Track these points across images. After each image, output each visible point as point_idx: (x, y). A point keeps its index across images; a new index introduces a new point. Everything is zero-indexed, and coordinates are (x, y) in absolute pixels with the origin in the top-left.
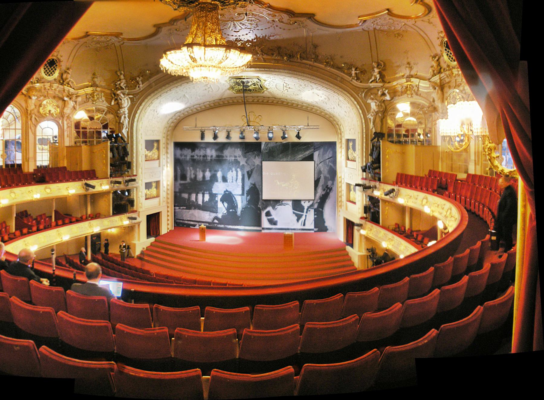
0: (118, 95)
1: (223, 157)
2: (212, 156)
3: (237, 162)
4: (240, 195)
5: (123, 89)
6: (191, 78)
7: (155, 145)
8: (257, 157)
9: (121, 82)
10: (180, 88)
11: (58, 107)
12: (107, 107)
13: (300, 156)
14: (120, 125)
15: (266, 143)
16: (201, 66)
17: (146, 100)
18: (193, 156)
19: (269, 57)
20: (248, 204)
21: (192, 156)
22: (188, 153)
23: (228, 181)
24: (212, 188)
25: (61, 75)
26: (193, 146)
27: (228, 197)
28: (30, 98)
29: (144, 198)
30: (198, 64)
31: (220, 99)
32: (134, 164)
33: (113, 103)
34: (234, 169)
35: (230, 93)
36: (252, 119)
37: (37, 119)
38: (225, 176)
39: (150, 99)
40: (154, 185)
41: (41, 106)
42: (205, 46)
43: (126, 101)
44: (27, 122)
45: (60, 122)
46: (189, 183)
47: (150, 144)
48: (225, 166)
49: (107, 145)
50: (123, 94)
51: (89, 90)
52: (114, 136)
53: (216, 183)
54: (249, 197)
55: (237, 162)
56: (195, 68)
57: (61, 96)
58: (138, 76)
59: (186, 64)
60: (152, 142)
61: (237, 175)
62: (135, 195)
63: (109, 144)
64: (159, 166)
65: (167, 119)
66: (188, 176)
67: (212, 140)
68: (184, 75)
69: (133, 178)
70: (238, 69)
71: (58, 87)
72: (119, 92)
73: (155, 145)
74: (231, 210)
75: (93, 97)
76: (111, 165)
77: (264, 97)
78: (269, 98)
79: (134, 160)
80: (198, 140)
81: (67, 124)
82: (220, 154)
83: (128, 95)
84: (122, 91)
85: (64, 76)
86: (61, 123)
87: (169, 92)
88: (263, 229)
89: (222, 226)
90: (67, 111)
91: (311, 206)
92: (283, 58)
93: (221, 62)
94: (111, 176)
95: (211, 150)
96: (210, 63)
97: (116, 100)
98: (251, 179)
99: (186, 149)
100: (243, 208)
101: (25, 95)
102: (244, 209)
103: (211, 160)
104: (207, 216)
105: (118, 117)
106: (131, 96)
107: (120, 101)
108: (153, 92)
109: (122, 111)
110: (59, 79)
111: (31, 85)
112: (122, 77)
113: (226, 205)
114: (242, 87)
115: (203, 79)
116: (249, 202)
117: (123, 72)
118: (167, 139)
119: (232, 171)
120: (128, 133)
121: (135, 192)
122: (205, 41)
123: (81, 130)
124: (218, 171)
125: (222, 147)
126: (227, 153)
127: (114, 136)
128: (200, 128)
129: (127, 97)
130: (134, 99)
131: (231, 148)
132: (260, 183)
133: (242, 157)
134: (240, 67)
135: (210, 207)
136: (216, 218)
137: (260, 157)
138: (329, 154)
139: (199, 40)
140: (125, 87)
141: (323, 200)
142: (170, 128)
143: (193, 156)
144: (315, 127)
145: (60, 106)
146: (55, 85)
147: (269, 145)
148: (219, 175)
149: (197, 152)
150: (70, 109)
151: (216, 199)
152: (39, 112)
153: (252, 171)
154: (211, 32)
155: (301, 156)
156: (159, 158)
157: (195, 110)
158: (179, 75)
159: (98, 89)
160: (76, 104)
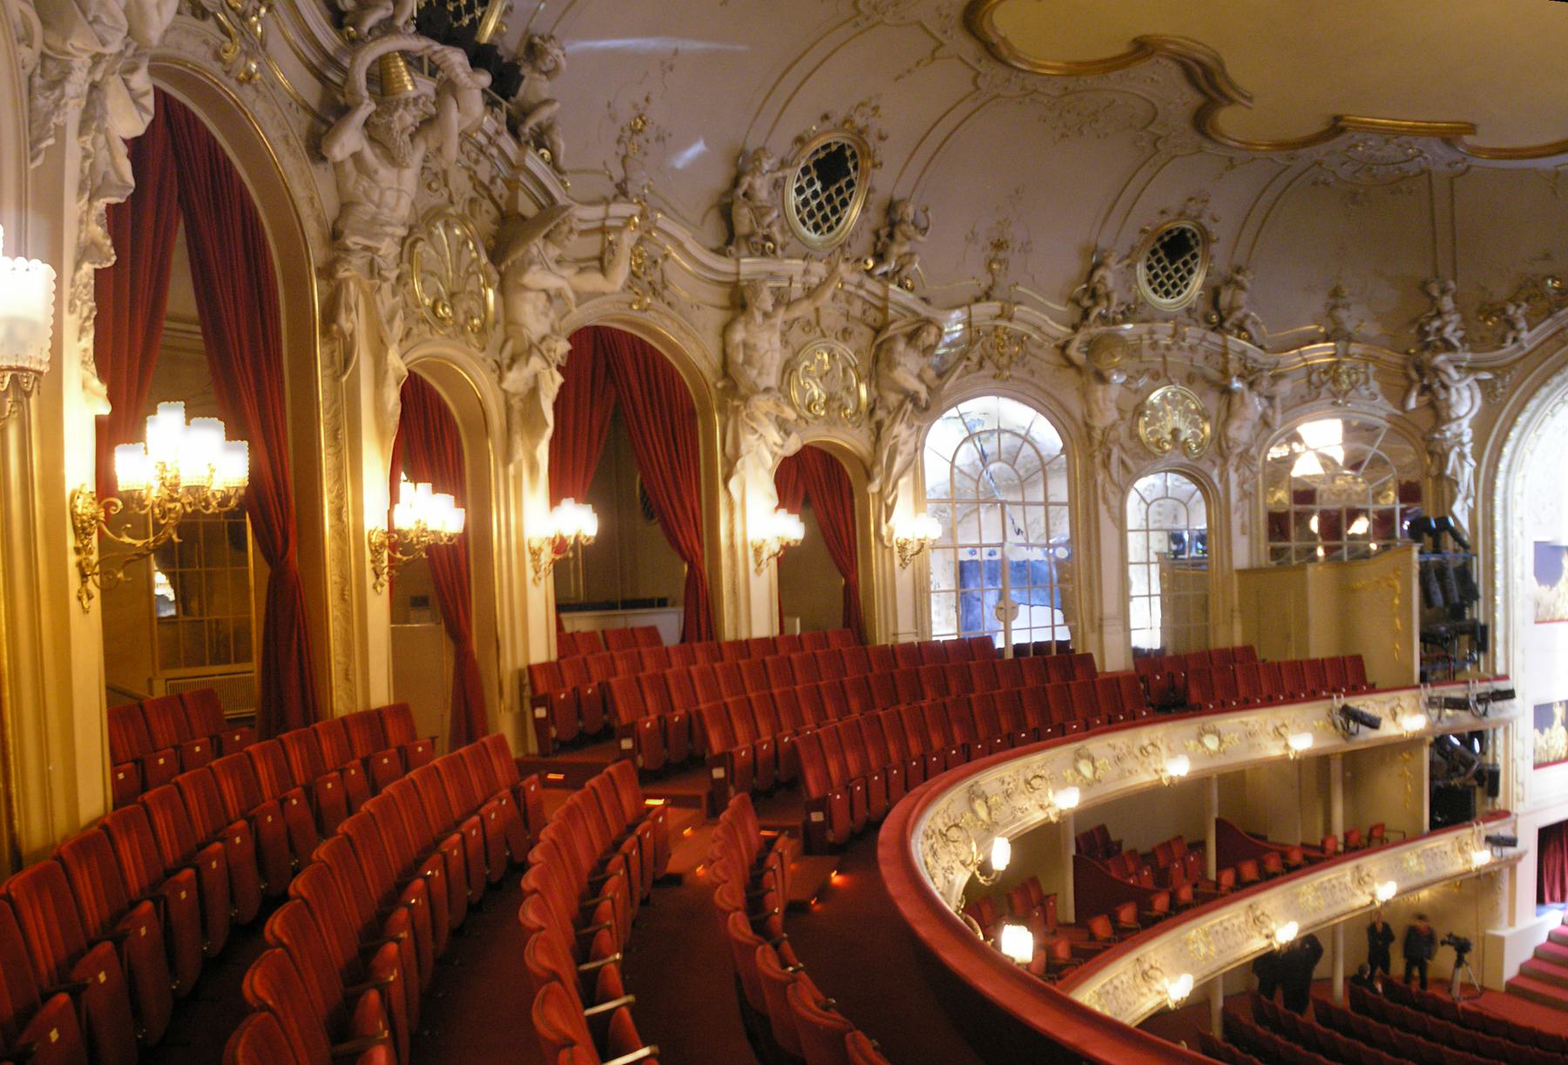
11: (1206, 418)
12: (1390, 418)
14: (1446, 486)
25: (1213, 294)
28: (1102, 378)
33: (1412, 403)
37: (1129, 462)
41: (1142, 414)
44: (1089, 476)
45: (1215, 474)
49: (1409, 564)
57: (1213, 374)
71: (1203, 339)
81: (1241, 484)
85: (1225, 299)
86: (1216, 480)
90: (1240, 432)
101: (1079, 370)
105: (1431, 453)
109: (1449, 431)
110: (1203, 307)
111: (1103, 329)
120: (1472, 515)
145: (1214, 413)
146: (1193, 333)
150: (1249, 424)
152: (1133, 435)
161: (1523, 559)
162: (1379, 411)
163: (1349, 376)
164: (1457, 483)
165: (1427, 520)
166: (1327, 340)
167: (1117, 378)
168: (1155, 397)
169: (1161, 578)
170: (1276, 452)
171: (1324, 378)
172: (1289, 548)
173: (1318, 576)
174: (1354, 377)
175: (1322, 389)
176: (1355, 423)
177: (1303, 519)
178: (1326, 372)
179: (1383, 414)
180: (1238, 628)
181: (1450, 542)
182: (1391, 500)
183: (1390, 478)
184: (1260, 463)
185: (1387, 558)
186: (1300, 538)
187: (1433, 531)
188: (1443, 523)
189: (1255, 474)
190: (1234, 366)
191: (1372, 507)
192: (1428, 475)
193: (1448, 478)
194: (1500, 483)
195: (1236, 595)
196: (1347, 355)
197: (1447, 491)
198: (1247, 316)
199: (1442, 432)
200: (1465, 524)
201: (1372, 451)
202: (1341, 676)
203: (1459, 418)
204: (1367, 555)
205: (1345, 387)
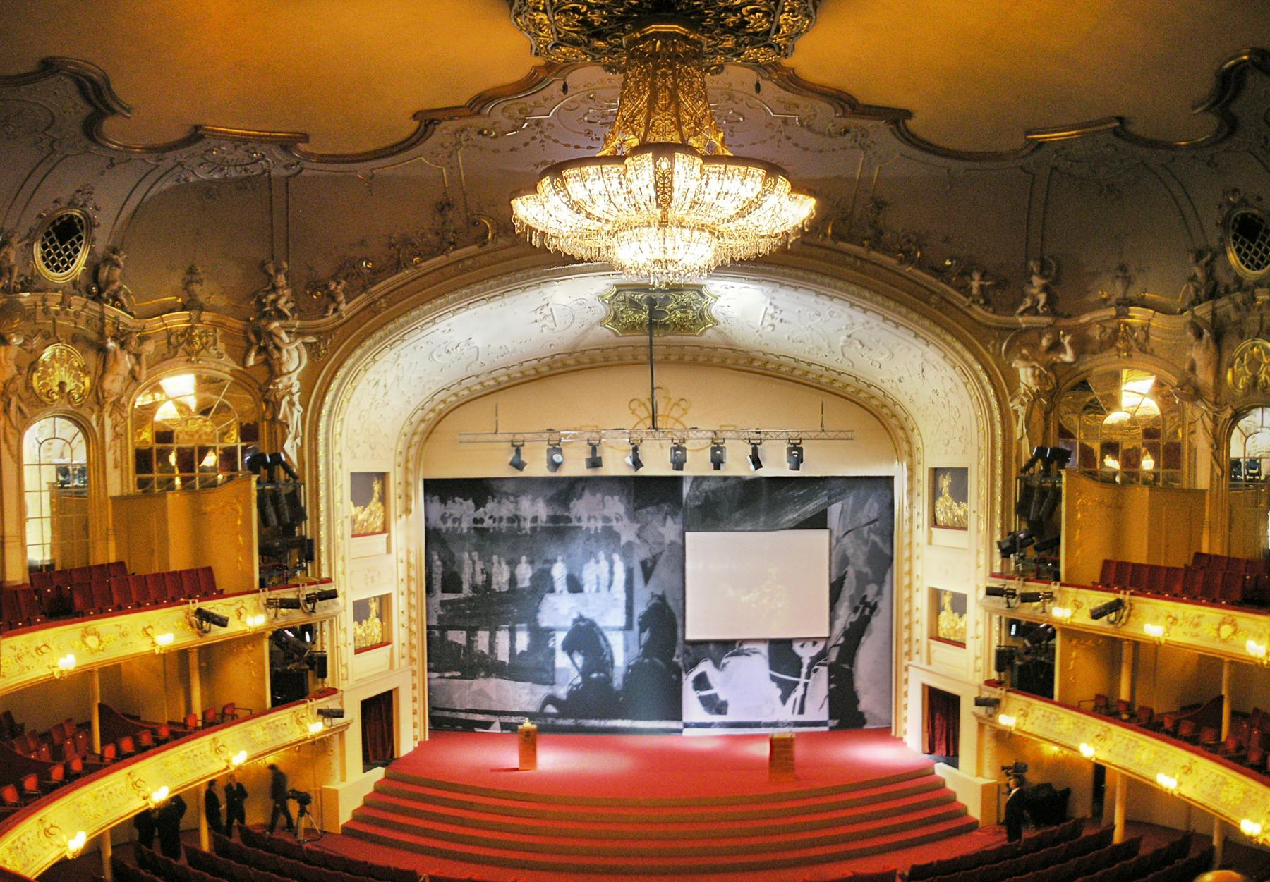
0: (271, 335)
1: (569, 520)
2: (535, 519)
3: (610, 535)
4: (620, 629)
5: (285, 317)
7: (377, 487)
8: (669, 520)
12: (233, 373)
13: (791, 516)
14: (279, 428)
17: (359, 352)
18: (482, 521)
20: (645, 655)
22: (463, 509)
23: (586, 589)
24: (537, 611)
26: (479, 490)
27: (585, 638)
31: (570, 354)
33: (251, 362)
34: (602, 555)
35: (605, 333)
38: (577, 574)
39: (370, 348)
40: (374, 606)
43: (295, 354)
46: (471, 599)
47: (367, 486)
48: (577, 547)
50: (286, 332)
53: (549, 598)
54: (646, 635)
55: (610, 535)
58: (334, 277)
60: (370, 476)
61: (611, 572)
64: (389, 551)
65: (411, 409)
66: (466, 577)
72: (275, 324)
73: (377, 487)
74: (595, 675)
78: (715, 349)
81: (114, 427)
83: (300, 333)
84: (283, 322)
88: (686, 726)
89: (570, 722)
91: (823, 655)
95: (534, 500)
97: (262, 350)
98: (652, 580)
100: (628, 667)
102: (633, 671)
103: (533, 529)
104: (522, 696)
105: (267, 402)
107: (276, 355)
109: (282, 383)
113: (579, 659)
116: (647, 649)
119: (598, 562)
120: (300, 450)
124: (555, 561)
125: (565, 491)
128: (510, 437)
129: (299, 341)
130: (318, 350)
131: (593, 494)
132: (679, 596)
133: (626, 520)
135: (529, 668)
136: (551, 700)
137: (679, 519)
138: (872, 509)
141: (855, 634)
142: (416, 438)
143: (482, 521)
144: (842, 435)
147: (706, 486)
148: (559, 572)
149: (491, 506)
151: (551, 645)
153: (655, 559)
155: (792, 516)
156: (385, 529)
162: (225, 367)
165: (263, 455)
167: (16, 341)
168: (47, 355)
169: (51, 503)
170: (142, 400)
171: (181, 340)
172: (152, 479)
173: (175, 502)
175: (180, 348)
176: (205, 376)
177: (163, 455)
179: (227, 369)
180: (112, 545)
181: (282, 473)
182: (234, 440)
183: (233, 422)
184: (129, 409)
185: (230, 487)
186: (161, 471)
187: (267, 464)
188: (276, 458)
189: (125, 419)
190: (109, 329)
191: (218, 446)
192: (263, 419)
193: (281, 423)
194: (322, 425)
195: (110, 521)
196: (199, 321)
197: (279, 431)
198: (120, 288)
200: (294, 459)
201: (219, 399)
202: (197, 584)
204: (214, 485)
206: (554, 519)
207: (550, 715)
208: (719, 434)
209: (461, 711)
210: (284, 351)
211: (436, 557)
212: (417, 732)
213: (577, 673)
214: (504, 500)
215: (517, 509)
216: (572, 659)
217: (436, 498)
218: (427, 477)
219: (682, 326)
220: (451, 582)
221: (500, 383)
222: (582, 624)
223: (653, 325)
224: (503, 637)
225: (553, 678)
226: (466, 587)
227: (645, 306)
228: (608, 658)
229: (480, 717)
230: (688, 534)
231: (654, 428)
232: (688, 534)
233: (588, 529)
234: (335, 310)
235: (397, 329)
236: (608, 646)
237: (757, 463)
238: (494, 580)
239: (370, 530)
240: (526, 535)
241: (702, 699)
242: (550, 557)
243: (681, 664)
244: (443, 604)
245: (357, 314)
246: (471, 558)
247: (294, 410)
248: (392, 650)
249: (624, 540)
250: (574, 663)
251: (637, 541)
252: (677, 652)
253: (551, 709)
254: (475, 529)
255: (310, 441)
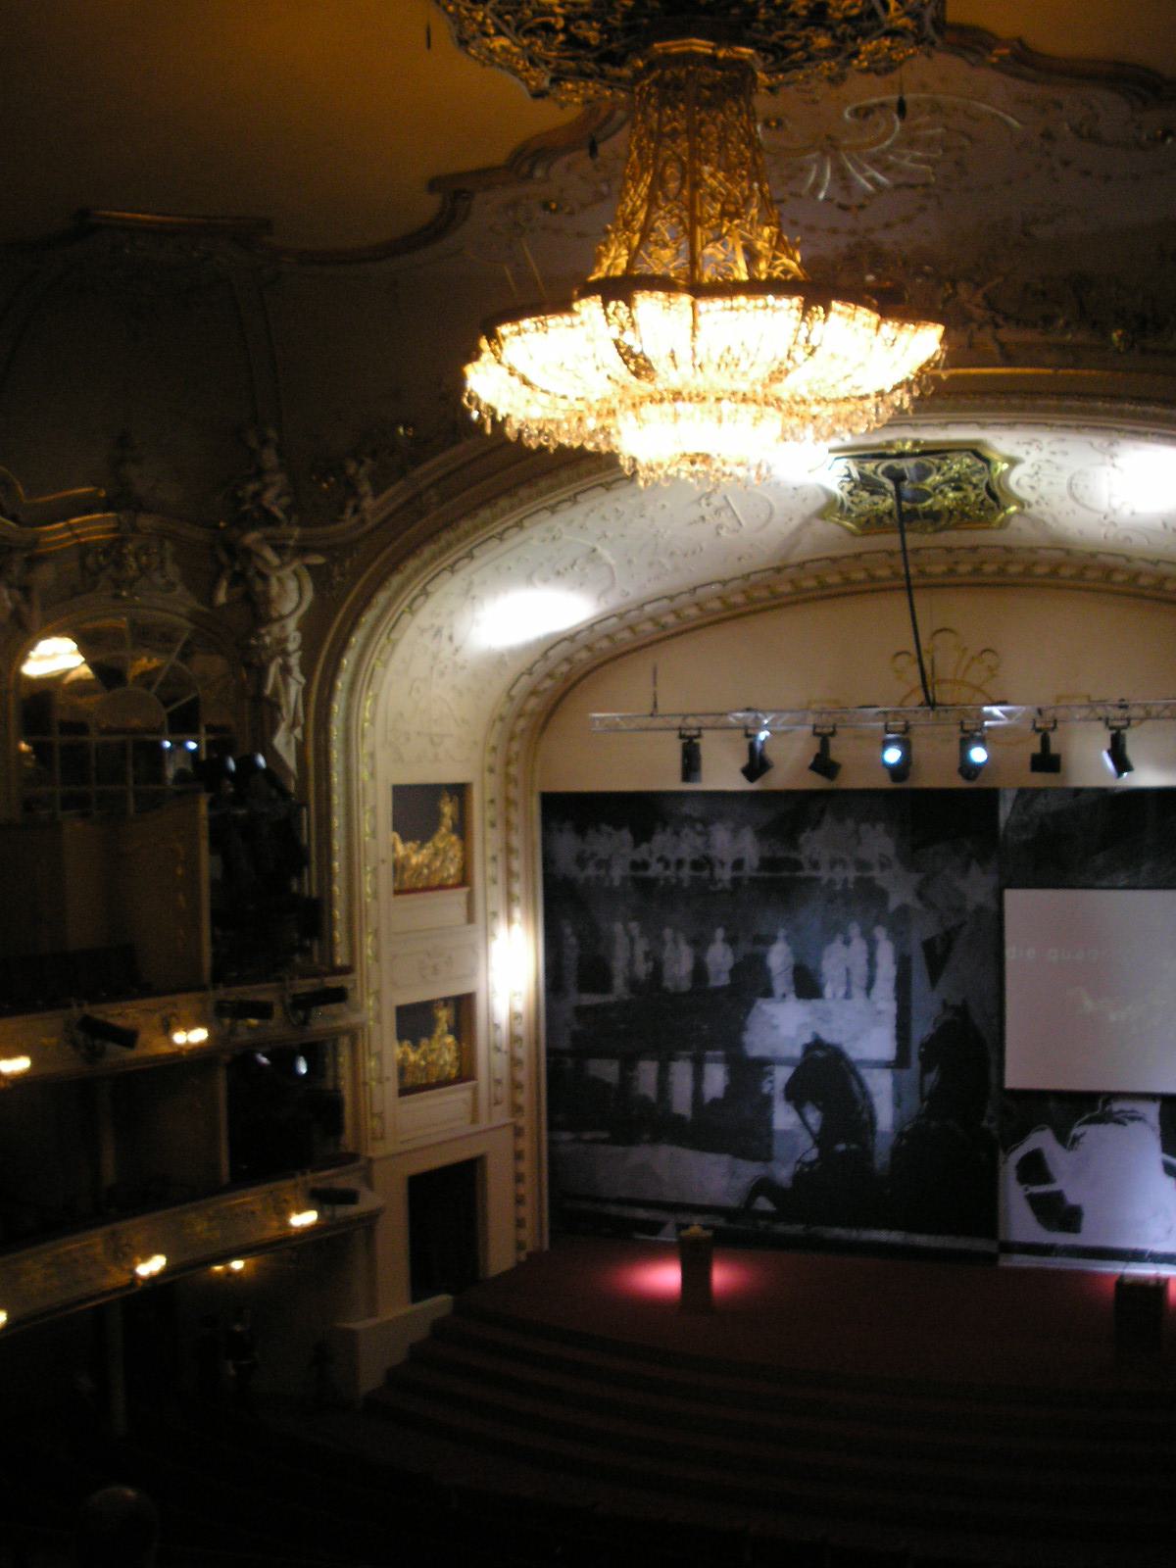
0: (248, 552)
1: (797, 865)
4: (886, 1065)
6: (624, 462)
7: (448, 809)
8: (975, 870)
9: (265, 487)
10: (575, 513)
14: (264, 712)
15: (1022, 792)
16: (677, 396)
17: (396, 580)
18: (645, 865)
19: (1030, 336)
21: (636, 865)
22: (615, 848)
23: (828, 991)
24: (742, 1028)
26: (640, 812)
27: (825, 1074)
29: (392, 1086)
30: (661, 384)
31: (779, 570)
32: (337, 913)
33: (221, 597)
34: (854, 930)
36: (946, 661)
39: (417, 572)
40: (444, 1015)
42: (699, 290)
43: (292, 585)
47: (421, 808)
51: (94, 527)
52: (232, 765)
53: (766, 1006)
54: (932, 1077)
55: (869, 895)
56: (649, 410)
59: (598, 389)
60: (430, 794)
61: (872, 963)
62: (345, 1071)
63: (203, 809)
66: (619, 965)
67: (738, 783)
68: (590, 446)
69: (333, 982)
70: (869, 404)
72: (252, 538)
75: (119, 564)
76: (217, 919)
77: (1008, 550)
79: (337, 889)
80: (670, 780)
82: (781, 854)
83: (302, 550)
84: (270, 531)
87: (515, 538)
88: (1009, 1248)
89: (797, 1229)
92: (1106, 335)
93: (779, 375)
94: (219, 977)
95: (735, 832)
96: (723, 382)
97: (238, 578)
99: (605, 828)
100: (901, 1135)
102: (909, 1138)
103: (735, 881)
104: (714, 1178)
105: (249, 666)
106: (318, 560)
107: (259, 586)
108: (431, 536)
112: (270, 458)
113: (814, 1117)
114: (890, 501)
115: (686, 466)
117: (272, 434)
118: (508, 779)
119: (847, 942)
120: (301, 748)
121: (344, 1059)
122: (693, 262)
123: (57, 739)
124: (770, 940)
125: (786, 815)
126: (815, 844)
127: (232, 765)
128: (677, 722)
129: (296, 564)
134: (880, 394)
136: (763, 1186)
139: (665, 260)
140: (287, 510)
142: (522, 723)
143: (645, 865)
147: (1040, 805)
148: (779, 958)
149: (661, 841)
153: (949, 938)
154: (724, 214)
156: (465, 879)
157: (648, 627)
158: (561, 447)
159: (146, 521)
160: (28, 599)
161: (374, 809)
163: (137, 558)
164: (277, 707)
166: (105, 510)
174: (144, 559)
178: (106, 553)
179: (182, 610)
194: (337, 707)
199: (259, 637)
200: (291, 762)
203: (282, 618)
205: (131, 573)
206: (767, 863)
207: (764, 1215)
208: (1049, 714)
209: (606, 1201)
210: (274, 581)
211: (568, 931)
212: (526, 1234)
213: (810, 1142)
214: (686, 830)
215: (707, 845)
216: (802, 1116)
217: (568, 825)
218: (547, 789)
219: (964, 514)
220: (595, 974)
221: (664, 627)
222: (820, 1054)
223: (906, 518)
224: (681, 1073)
225: (769, 1146)
226: (619, 982)
227: (890, 485)
228: (865, 1116)
229: (641, 1214)
230: (1010, 895)
231: (930, 703)
232: (1010, 895)
233: (831, 882)
234: (356, 510)
235: (459, 540)
236: (866, 1094)
237: (1122, 765)
238: (667, 973)
239: (436, 881)
240: (723, 891)
241: (1034, 1201)
242: (764, 931)
243: (995, 1133)
244: (580, 1012)
245: (391, 515)
246: (628, 932)
247: (291, 681)
248: (475, 1091)
249: (894, 903)
250: (805, 1123)
251: (918, 905)
252: (989, 1111)
253: (764, 1204)
254: (634, 879)
255: (317, 733)
